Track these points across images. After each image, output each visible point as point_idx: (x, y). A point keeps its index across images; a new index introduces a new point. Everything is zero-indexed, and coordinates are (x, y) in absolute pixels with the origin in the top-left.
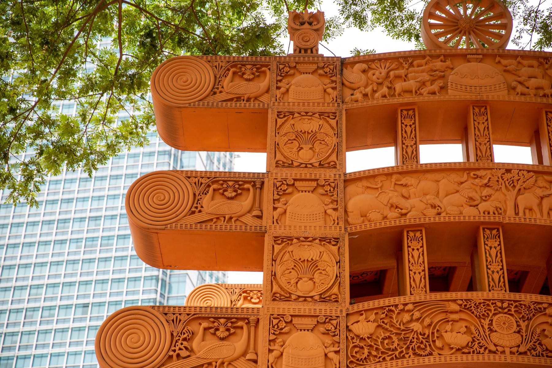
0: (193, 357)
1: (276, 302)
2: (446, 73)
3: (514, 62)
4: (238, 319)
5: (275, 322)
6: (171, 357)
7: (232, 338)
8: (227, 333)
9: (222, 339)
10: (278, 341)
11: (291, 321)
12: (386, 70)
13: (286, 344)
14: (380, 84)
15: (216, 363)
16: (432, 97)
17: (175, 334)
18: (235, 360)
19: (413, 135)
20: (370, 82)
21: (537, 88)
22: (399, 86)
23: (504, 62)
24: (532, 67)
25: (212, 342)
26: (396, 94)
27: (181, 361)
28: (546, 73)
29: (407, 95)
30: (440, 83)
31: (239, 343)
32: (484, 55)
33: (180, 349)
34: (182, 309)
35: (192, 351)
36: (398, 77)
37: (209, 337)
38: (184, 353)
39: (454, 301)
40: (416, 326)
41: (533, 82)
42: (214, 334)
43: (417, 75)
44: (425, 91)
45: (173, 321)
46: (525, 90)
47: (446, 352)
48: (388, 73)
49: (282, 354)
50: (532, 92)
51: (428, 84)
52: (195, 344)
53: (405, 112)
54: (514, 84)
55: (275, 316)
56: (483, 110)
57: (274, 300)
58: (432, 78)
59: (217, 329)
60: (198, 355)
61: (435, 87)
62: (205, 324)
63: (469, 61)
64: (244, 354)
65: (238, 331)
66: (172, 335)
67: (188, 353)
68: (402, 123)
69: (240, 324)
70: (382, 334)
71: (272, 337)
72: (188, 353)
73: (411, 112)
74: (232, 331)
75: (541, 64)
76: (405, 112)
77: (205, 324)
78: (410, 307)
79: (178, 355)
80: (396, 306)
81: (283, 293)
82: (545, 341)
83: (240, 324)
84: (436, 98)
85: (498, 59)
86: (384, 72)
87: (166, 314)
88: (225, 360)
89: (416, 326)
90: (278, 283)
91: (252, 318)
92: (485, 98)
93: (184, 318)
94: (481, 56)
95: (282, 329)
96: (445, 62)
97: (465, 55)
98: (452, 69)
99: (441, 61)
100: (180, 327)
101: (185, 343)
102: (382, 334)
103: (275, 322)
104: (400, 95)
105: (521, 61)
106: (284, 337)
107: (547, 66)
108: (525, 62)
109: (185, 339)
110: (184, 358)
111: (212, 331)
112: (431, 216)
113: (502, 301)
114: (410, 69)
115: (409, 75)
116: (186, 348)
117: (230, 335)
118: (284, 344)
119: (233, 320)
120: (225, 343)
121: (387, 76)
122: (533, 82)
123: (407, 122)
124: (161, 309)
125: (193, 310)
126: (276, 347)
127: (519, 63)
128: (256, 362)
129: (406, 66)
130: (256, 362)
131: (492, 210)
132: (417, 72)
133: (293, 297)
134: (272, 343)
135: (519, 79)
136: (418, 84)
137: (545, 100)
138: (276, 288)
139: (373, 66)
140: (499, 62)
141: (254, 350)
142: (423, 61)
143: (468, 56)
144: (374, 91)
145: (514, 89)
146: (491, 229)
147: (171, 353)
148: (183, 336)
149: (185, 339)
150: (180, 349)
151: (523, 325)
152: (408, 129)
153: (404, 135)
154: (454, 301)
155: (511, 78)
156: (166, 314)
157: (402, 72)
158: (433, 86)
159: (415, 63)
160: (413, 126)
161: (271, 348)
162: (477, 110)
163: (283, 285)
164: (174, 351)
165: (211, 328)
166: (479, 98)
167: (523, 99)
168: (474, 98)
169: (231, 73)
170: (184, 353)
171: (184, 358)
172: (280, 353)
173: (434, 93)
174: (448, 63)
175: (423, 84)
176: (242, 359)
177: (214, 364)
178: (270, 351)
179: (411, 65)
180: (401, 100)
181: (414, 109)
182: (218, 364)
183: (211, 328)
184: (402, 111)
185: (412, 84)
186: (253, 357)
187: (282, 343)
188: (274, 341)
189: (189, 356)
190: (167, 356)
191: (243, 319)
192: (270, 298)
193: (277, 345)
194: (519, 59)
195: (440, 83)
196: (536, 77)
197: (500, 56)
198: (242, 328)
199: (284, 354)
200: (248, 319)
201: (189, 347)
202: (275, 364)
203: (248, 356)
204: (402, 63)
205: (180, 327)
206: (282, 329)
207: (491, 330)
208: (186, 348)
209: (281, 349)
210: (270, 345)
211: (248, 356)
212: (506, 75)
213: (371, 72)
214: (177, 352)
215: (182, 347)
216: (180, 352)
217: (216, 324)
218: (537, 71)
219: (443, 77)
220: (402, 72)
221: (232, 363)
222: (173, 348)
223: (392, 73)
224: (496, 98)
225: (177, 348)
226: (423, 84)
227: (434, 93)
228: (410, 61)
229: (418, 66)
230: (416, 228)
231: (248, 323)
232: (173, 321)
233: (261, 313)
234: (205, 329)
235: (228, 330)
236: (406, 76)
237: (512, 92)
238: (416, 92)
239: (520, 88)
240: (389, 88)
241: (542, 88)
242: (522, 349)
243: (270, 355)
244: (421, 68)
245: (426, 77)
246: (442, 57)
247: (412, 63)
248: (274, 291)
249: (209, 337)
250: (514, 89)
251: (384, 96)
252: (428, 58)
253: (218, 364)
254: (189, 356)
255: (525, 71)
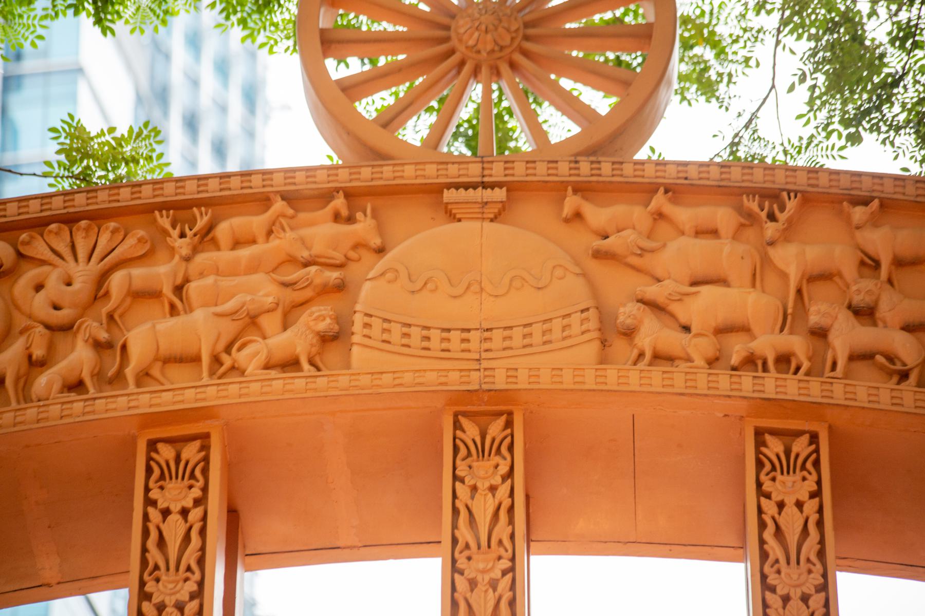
2: (354, 270)
3: (638, 214)
12: (95, 267)
14: (67, 328)
16: (279, 382)
19: (191, 557)
20: (21, 321)
21: (723, 331)
22: (143, 337)
23: (598, 215)
24: (714, 233)
26: (130, 372)
28: (766, 261)
29: (178, 375)
30: (319, 317)
32: (512, 188)
36: (143, 295)
41: (705, 307)
43: (227, 283)
44: (251, 355)
46: (671, 340)
48: (104, 276)
50: (700, 347)
51: (270, 322)
53: (166, 453)
54: (628, 312)
56: (495, 429)
58: (291, 296)
61: (296, 339)
63: (453, 217)
68: (150, 502)
73: (191, 452)
75: (750, 218)
76: (166, 453)
84: (297, 383)
85: (571, 202)
86: (83, 273)
92: (500, 382)
94: (500, 194)
96: (350, 220)
97: (434, 191)
98: (381, 251)
99: (337, 217)
104: (144, 376)
105: (669, 209)
107: (771, 229)
108: (684, 215)
114: (202, 259)
115: (193, 288)
121: (99, 290)
122: (705, 307)
123: (175, 495)
127: (660, 216)
129: (183, 246)
132: (233, 271)
135: (653, 291)
136: (229, 328)
137: (747, 381)
139: (39, 249)
140: (578, 216)
142: (256, 222)
143: (449, 195)
144: (36, 365)
145: (629, 333)
152: (174, 529)
153: (154, 555)
155: (621, 289)
157: (161, 272)
158: (289, 333)
159: (223, 230)
160: (195, 514)
162: (471, 431)
166: (474, 381)
167: (657, 376)
168: (455, 381)
173: (291, 364)
174: (364, 227)
175: (252, 322)
179: (206, 238)
180: (146, 401)
181: (206, 436)
184: (152, 445)
185: (199, 327)
194: (659, 200)
195: (319, 317)
196: (721, 281)
197: (581, 189)
204: (165, 233)
212: (596, 268)
213: (30, 275)
218: (729, 254)
219: (340, 287)
220: (161, 272)
223: (117, 281)
224: (546, 380)
226: (252, 322)
227: (291, 364)
228: (201, 223)
229: (237, 244)
236: (179, 290)
237: (619, 346)
238: (216, 360)
239: (652, 333)
240: (99, 346)
241: (744, 329)
244: (245, 253)
245: (264, 291)
246: (339, 202)
247: (210, 228)
250: (629, 333)
251: (77, 386)
252: (279, 205)
255: (680, 255)
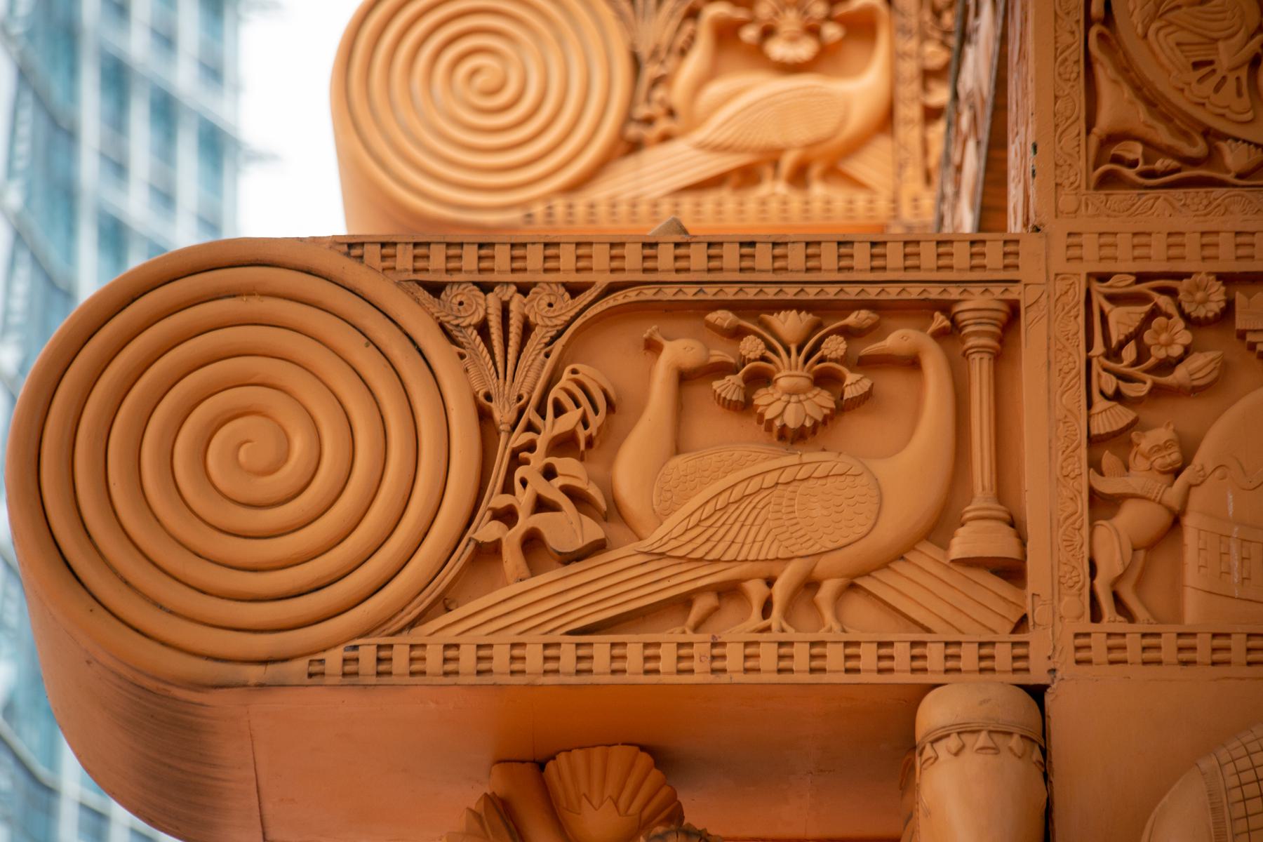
0: (623, 555)
1: (1120, 197)
5: (1122, 320)
6: (488, 553)
7: (857, 428)
8: (825, 399)
9: (795, 437)
10: (1146, 442)
11: (1228, 311)
13: (1203, 457)
15: (770, 582)
17: (502, 413)
18: (885, 565)
25: (731, 458)
27: (552, 579)
31: (900, 459)
33: (541, 505)
34: (534, 257)
35: (613, 512)
37: (711, 425)
38: (565, 530)
42: (745, 407)
45: (483, 329)
49: (1176, 522)
52: (631, 468)
55: (1121, 284)
57: (1107, 181)
59: (759, 379)
60: (652, 540)
62: (682, 349)
64: (939, 527)
65: (893, 384)
66: (484, 416)
67: (592, 531)
69: (898, 339)
71: (1109, 418)
72: (592, 531)
74: (854, 383)
77: (682, 349)
79: (532, 542)
81: (1163, 135)
83: (898, 339)
87: (435, 289)
88: (823, 565)
90: (1126, 70)
91: (976, 304)
93: (549, 311)
95: (1167, 366)
100: (532, 371)
101: (568, 467)
103: (1122, 320)
106: (1187, 414)
109: (564, 445)
110: (569, 559)
111: (729, 387)
116: (577, 497)
117: (843, 408)
118: (1186, 462)
119: (855, 318)
120: (811, 458)
124: (404, 258)
125: (600, 257)
126: (1138, 479)
128: (1011, 571)
130: (1011, 571)
133: (1234, 158)
134: (1108, 459)
138: (1115, 104)
141: (1000, 497)
147: (487, 531)
148: (552, 427)
149: (564, 445)
150: (541, 505)
156: (435, 289)
161: (1108, 486)
163: (1163, 85)
164: (507, 516)
165: (721, 370)
170: (565, 530)
171: (569, 559)
172: (1163, 518)
176: (927, 556)
177: (756, 590)
178: (1102, 504)
182: (779, 593)
183: (721, 370)
186: (1000, 544)
187: (1174, 456)
188: (1120, 440)
189: (598, 547)
190: (465, 552)
191: (920, 309)
192: (1080, 170)
193: (1139, 464)
198: (912, 363)
199: (1190, 522)
200: (945, 307)
201: (594, 491)
202: (1139, 586)
203: (963, 543)
205: (532, 371)
206: (1167, 366)
208: (577, 497)
209: (1173, 495)
210: (1095, 465)
211: (963, 543)
214: (525, 521)
215: (552, 491)
216: (542, 521)
217: (751, 347)
221: (865, 583)
222: (501, 501)
225: (523, 500)
231: (950, 334)
232: (483, 329)
233: (1029, 269)
234: (685, 378)
235: (826, 379)
243: (1104, 530)
248: (1105, 120)
249: (711, 425)
253: (779, 593)
254: (598, 547)
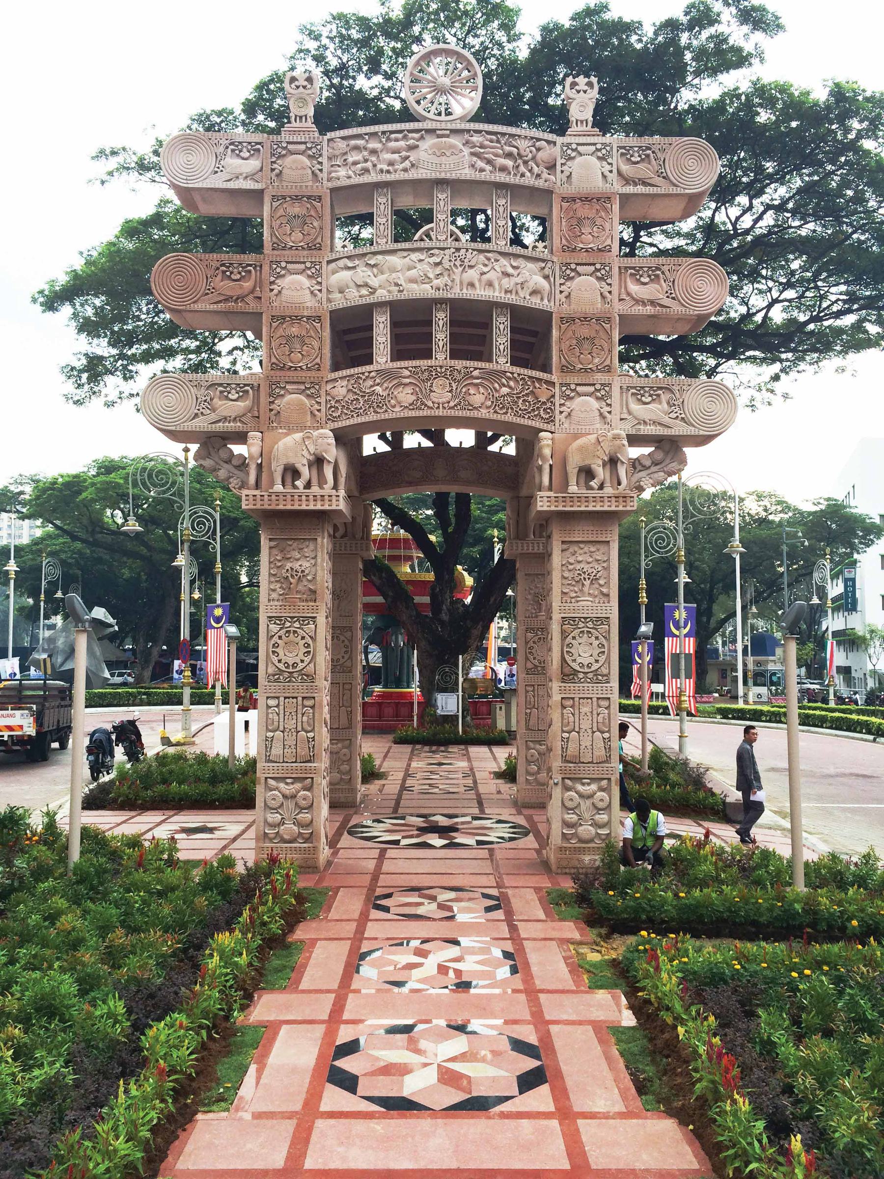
4: (245, 385)
39: (406, 368)
40: (378, 389)
47: (397, 409)
70: (351, 396)
78: (373, 374)
80: (363, 373)
82: (468, 398)
89: (378, 389)
102: (351, 396)
112: (395, 296)
113: (441, 367)
131: (442, 286)
146: (441, 304)
151: (454, 385)
154: (406, 368)
169: (229, 150)
207: (431, 391)
230: (381, 304)
242: (452, 404)
